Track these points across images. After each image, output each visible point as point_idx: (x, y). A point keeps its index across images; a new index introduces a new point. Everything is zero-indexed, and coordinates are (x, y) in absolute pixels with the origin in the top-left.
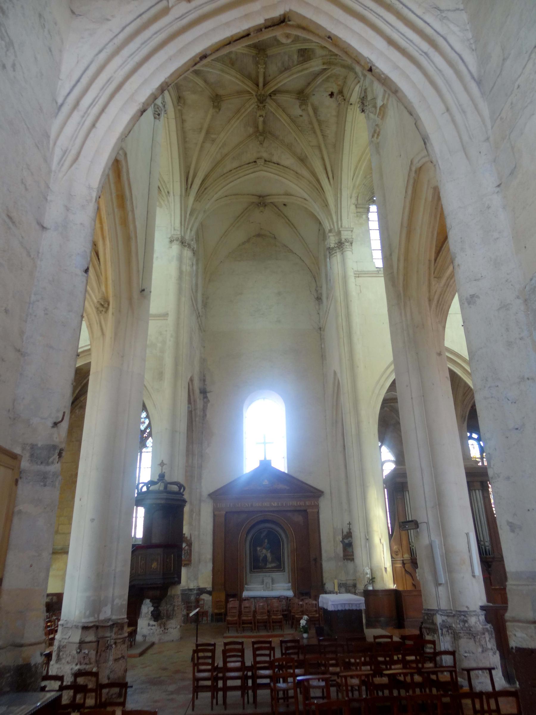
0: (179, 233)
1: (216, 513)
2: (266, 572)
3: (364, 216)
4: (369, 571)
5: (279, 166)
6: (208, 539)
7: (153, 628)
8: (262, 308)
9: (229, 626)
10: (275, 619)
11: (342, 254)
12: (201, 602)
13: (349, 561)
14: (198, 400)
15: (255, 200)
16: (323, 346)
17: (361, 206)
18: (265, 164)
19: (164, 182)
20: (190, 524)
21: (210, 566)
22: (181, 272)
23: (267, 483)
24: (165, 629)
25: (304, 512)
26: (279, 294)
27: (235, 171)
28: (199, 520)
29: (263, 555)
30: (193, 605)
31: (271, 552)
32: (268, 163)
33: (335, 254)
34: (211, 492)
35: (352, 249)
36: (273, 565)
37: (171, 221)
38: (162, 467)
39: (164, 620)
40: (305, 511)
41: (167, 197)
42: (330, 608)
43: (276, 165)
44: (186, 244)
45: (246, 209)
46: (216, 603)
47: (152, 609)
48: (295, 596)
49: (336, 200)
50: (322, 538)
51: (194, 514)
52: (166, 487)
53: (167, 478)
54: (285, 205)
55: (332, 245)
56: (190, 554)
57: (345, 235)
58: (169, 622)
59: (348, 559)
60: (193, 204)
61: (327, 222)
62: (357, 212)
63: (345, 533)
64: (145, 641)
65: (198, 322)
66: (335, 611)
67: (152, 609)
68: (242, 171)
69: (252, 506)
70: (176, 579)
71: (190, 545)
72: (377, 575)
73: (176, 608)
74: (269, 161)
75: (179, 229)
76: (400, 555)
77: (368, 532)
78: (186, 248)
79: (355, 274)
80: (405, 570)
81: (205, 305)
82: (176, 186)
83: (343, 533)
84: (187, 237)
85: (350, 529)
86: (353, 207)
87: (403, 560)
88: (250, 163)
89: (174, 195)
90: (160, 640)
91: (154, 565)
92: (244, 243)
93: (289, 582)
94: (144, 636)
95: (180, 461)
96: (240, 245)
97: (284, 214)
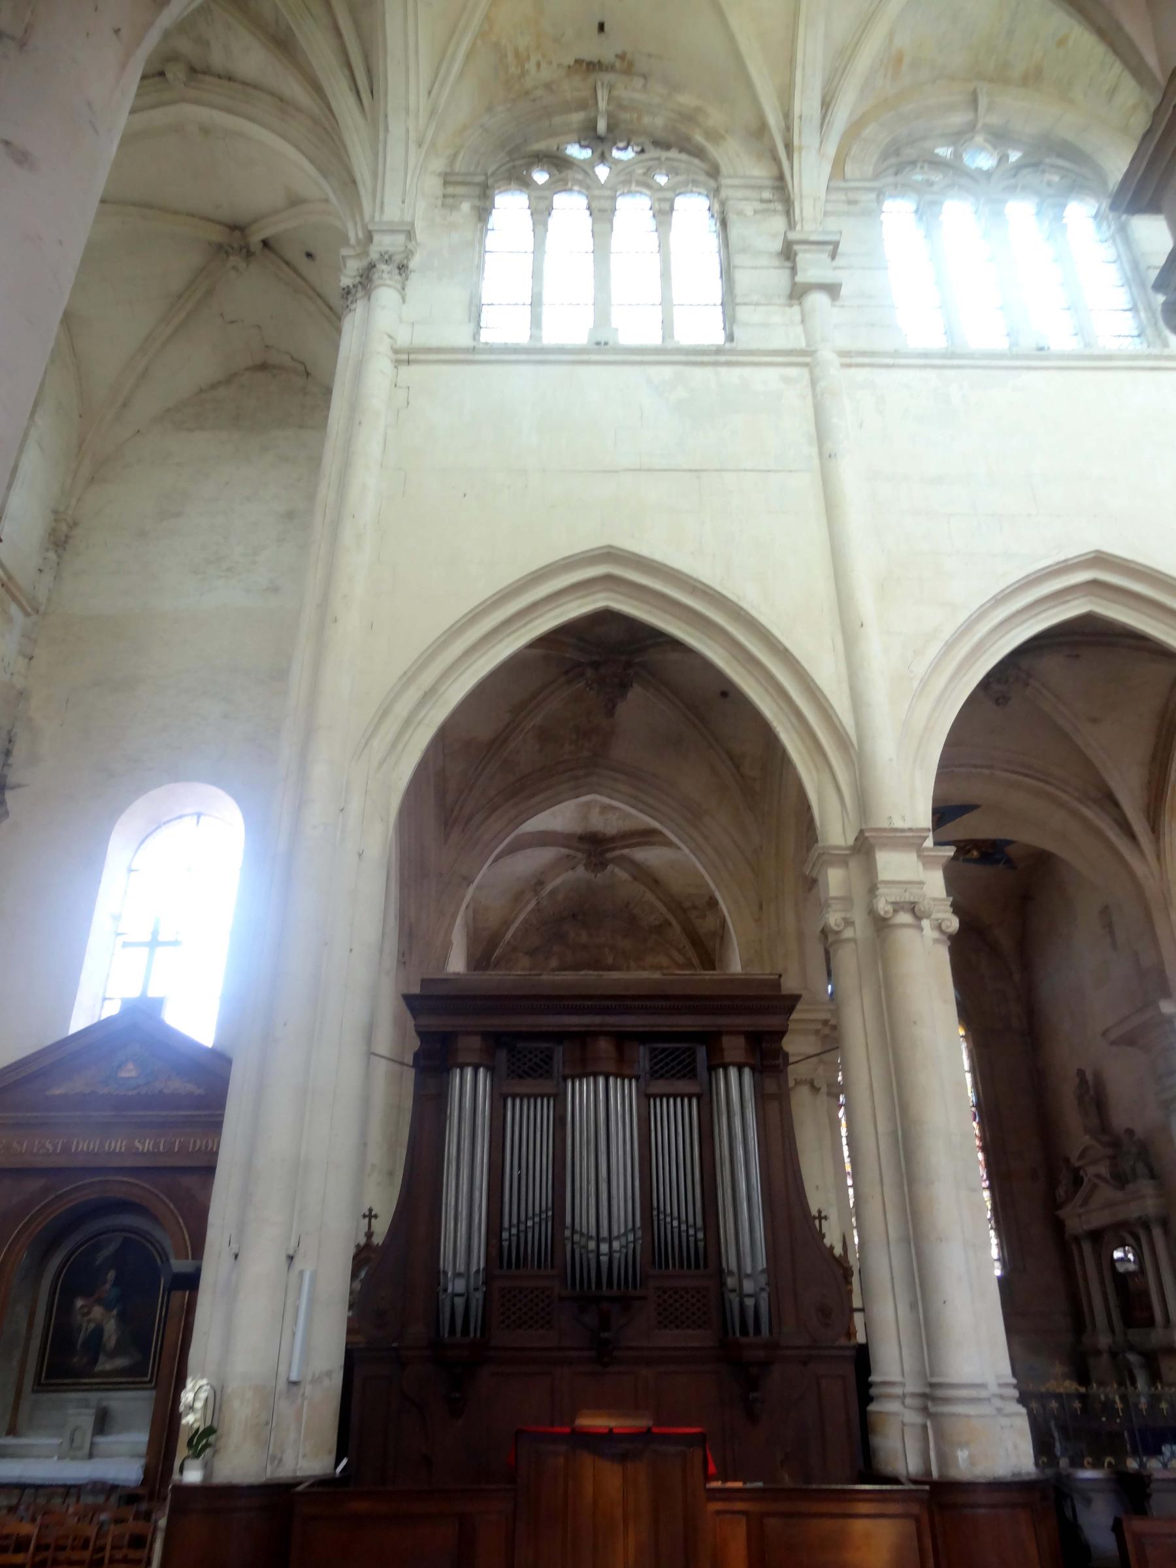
2: (91, 1388)
15: (216, 235)
23: (133, 1074)
29: (92, 1326)
31: (122, 1318)
32: (200, 76)
36: (121, 1362)
43: (225, 82)
62: (444, 196)
69: (66, 1149)
79: (396, 351)
92: (213, 387)
96: (201, 391)
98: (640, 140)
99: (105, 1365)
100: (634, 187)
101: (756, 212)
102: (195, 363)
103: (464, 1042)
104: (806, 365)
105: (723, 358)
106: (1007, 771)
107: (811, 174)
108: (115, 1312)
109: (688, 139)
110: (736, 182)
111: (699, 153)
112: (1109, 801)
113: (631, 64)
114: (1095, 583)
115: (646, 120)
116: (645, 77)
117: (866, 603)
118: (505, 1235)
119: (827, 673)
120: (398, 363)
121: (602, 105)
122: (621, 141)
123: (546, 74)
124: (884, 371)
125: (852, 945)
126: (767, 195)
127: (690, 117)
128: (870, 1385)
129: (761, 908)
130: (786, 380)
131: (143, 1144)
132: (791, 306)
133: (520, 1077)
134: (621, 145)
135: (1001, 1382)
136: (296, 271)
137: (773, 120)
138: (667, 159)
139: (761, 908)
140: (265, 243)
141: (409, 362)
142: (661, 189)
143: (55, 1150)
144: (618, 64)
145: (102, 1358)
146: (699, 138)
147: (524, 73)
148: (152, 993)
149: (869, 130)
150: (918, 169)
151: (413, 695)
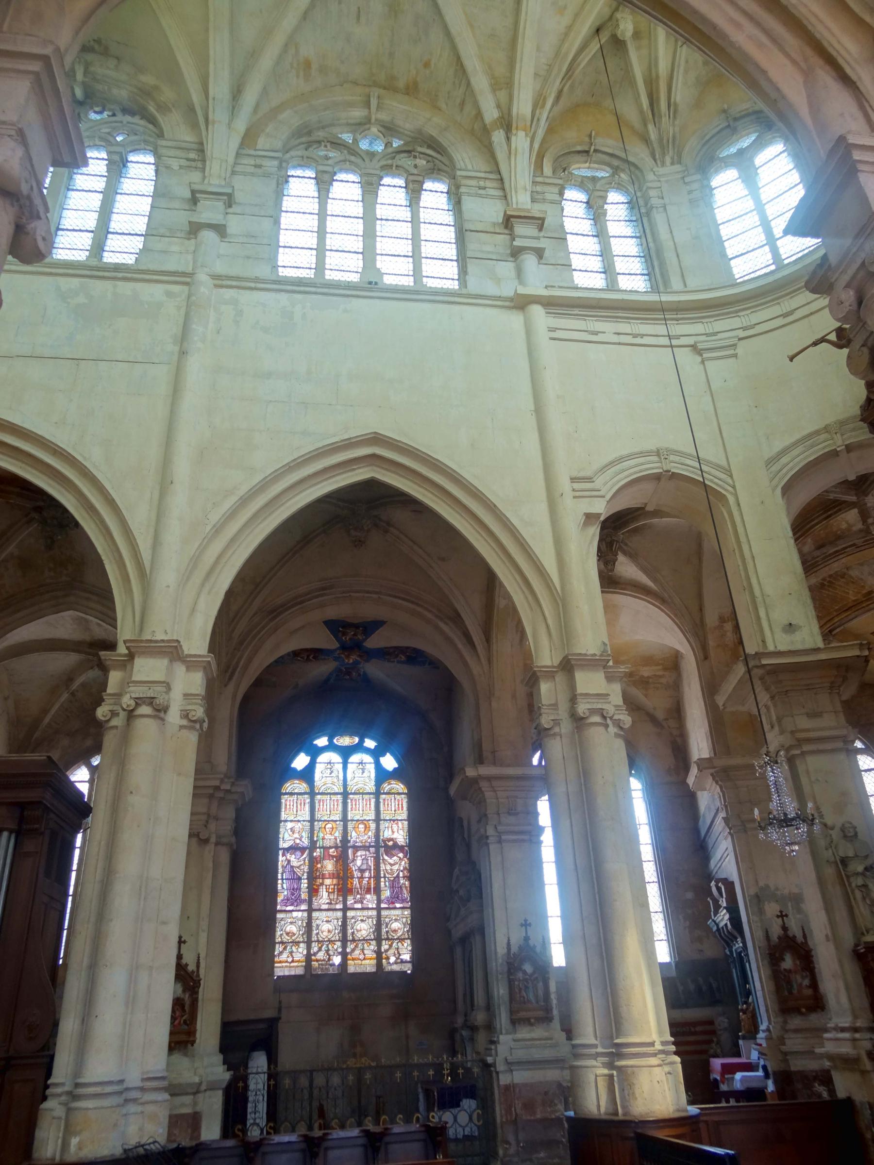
98: (112, 107)
100: (98, 142)
101: (181, 167)
104: (187, 284)
105: (120, 275)
106: (390, 595)
107: (223, 143)
110: (170, 144)
111: (152, 121)
112: (456, 619)
113: (106, 49)
114: (374, 456)
115: (115, 91)
116: (118, 58)
117: (182, 468)
119: (139, 519)
122: (98, 106)
124: (248, 292)
125: (114, 731)
126: (192, 155)
127: (147, 93)
128: (47, 1087)
130: (169, 294)
132: (189, 239)
134: (97, 109)
135: (145, 1077)
137: (196, 98)
138: (128, 123)
142: (118, 144)
144: (96, 47)
146: (152, 109)
149: (285, 115)
150: (322, 148)
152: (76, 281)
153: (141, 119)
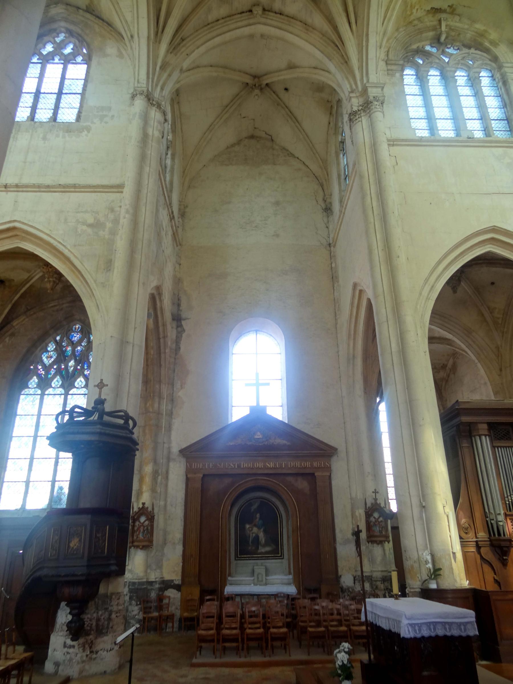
0: (145, 86)
1: (189, 476)
2: (258, 559)
3: (398, 75)
4: (429, 558)
5: (281, 16)
6: (177, 511)
7: (71, 650)
8: (256, 219)
9: (204, 645)
10: (275, 633)
11: (370, 117)
12: (166, 601)
13: (375, 545)
14: (169, 327)
15: (248, 79)
16: (333, 265)
17: (393, 62)
18: (263, 14)
19: (126, 22)
20: (153, 490)
21: (179, 549)
22: (144, 138)
23: (261, 437)
24: (91, 652)
25: (310, 476)
26: (277, 203)
27: (223, 21)
28: (166, 486)
29: (254, 535)
30: (154, 604)
31: (265, 531)
32: (267, 13)
33: (360, 119)
34: (184, 446)
35: (383, 110)
36: (268, 549)
37: (134, 73)
38: (101, 389)
39: (91, 637)
40: (313, 475)
41: (130, 41)
42: (406, 632)
43: (278, 15)
44: (154, 103)
45: (238, 95)
46: (186, 603)
47: (70, 617)
48: (299, 593)
49: (360, 52)
50: (335, 511)
51: (160, 477)
52: (101, 417)
53: (108, 408)
54: (286, 89)
55: (355, 109)
56: (150, 531)
57: (372, 92)
58: (99, 640)
59: (373, 542)
60: (165, 56)
61: (346, 82)
62: (388, 70)
63: (369, 505)
64: (56, 672)
65: (172, 227)
66: (415, 639)
67: (70, 617)
68: (235, 21)
69: (239, 466)
70: (114, 568)
71: (151, 518)
72: (443, 564)
73: (113, 616)
74: (269, 11)
75: (145, 82)
76: (471, 534)
77: (424, 496)
78: (154, 108)
79: (388, 140)
80: (482, 558)
81: (183, 214)
82: (141, 26)
83: (366, 504)
84: (157, 94)
85: (376, 499)
86: (382, 64)
87: (477, 542)
88: (243, 12)
89: (138, 37)
90: (81, 672)
91: (74, 543)
92: (233, 145)
93: (290, 573)
94: (57, 664)
95: (133, 386)
96: (228, 148)
97: (284, 104)
99: (262, 550)
102: (226, 136)
103: (480, 426)
108: (262, 530)
109: (481, 44)
113: (454, 10)
118: (507, 499)
120: (389, 145)
121: (443, 28)
122: (449, 44)
123: (420, 14)
127: (482, 35)
129: (501, 370)
131: (270, 464)
133: (499, 439)
134: (449, 46)
136: (277, 96)
138: (472, 53)
139: (501, 370)
140: (267, 85)
141: (393, 145)
143: (235, 467)
144: (448, 10)
145: (260, 547)
146: (487, 44)
147: (412, 13)
148: (261, 404)
151: (427, 288)
152: (500, 150)
153: (476, 50)
